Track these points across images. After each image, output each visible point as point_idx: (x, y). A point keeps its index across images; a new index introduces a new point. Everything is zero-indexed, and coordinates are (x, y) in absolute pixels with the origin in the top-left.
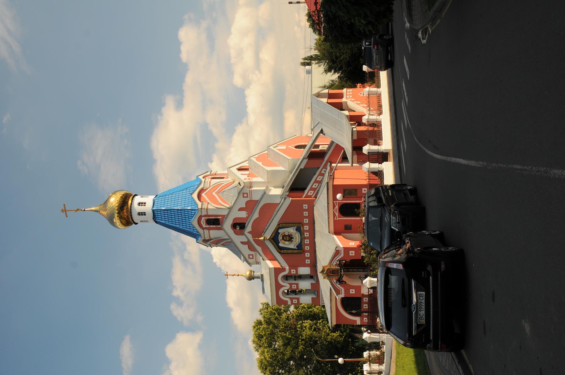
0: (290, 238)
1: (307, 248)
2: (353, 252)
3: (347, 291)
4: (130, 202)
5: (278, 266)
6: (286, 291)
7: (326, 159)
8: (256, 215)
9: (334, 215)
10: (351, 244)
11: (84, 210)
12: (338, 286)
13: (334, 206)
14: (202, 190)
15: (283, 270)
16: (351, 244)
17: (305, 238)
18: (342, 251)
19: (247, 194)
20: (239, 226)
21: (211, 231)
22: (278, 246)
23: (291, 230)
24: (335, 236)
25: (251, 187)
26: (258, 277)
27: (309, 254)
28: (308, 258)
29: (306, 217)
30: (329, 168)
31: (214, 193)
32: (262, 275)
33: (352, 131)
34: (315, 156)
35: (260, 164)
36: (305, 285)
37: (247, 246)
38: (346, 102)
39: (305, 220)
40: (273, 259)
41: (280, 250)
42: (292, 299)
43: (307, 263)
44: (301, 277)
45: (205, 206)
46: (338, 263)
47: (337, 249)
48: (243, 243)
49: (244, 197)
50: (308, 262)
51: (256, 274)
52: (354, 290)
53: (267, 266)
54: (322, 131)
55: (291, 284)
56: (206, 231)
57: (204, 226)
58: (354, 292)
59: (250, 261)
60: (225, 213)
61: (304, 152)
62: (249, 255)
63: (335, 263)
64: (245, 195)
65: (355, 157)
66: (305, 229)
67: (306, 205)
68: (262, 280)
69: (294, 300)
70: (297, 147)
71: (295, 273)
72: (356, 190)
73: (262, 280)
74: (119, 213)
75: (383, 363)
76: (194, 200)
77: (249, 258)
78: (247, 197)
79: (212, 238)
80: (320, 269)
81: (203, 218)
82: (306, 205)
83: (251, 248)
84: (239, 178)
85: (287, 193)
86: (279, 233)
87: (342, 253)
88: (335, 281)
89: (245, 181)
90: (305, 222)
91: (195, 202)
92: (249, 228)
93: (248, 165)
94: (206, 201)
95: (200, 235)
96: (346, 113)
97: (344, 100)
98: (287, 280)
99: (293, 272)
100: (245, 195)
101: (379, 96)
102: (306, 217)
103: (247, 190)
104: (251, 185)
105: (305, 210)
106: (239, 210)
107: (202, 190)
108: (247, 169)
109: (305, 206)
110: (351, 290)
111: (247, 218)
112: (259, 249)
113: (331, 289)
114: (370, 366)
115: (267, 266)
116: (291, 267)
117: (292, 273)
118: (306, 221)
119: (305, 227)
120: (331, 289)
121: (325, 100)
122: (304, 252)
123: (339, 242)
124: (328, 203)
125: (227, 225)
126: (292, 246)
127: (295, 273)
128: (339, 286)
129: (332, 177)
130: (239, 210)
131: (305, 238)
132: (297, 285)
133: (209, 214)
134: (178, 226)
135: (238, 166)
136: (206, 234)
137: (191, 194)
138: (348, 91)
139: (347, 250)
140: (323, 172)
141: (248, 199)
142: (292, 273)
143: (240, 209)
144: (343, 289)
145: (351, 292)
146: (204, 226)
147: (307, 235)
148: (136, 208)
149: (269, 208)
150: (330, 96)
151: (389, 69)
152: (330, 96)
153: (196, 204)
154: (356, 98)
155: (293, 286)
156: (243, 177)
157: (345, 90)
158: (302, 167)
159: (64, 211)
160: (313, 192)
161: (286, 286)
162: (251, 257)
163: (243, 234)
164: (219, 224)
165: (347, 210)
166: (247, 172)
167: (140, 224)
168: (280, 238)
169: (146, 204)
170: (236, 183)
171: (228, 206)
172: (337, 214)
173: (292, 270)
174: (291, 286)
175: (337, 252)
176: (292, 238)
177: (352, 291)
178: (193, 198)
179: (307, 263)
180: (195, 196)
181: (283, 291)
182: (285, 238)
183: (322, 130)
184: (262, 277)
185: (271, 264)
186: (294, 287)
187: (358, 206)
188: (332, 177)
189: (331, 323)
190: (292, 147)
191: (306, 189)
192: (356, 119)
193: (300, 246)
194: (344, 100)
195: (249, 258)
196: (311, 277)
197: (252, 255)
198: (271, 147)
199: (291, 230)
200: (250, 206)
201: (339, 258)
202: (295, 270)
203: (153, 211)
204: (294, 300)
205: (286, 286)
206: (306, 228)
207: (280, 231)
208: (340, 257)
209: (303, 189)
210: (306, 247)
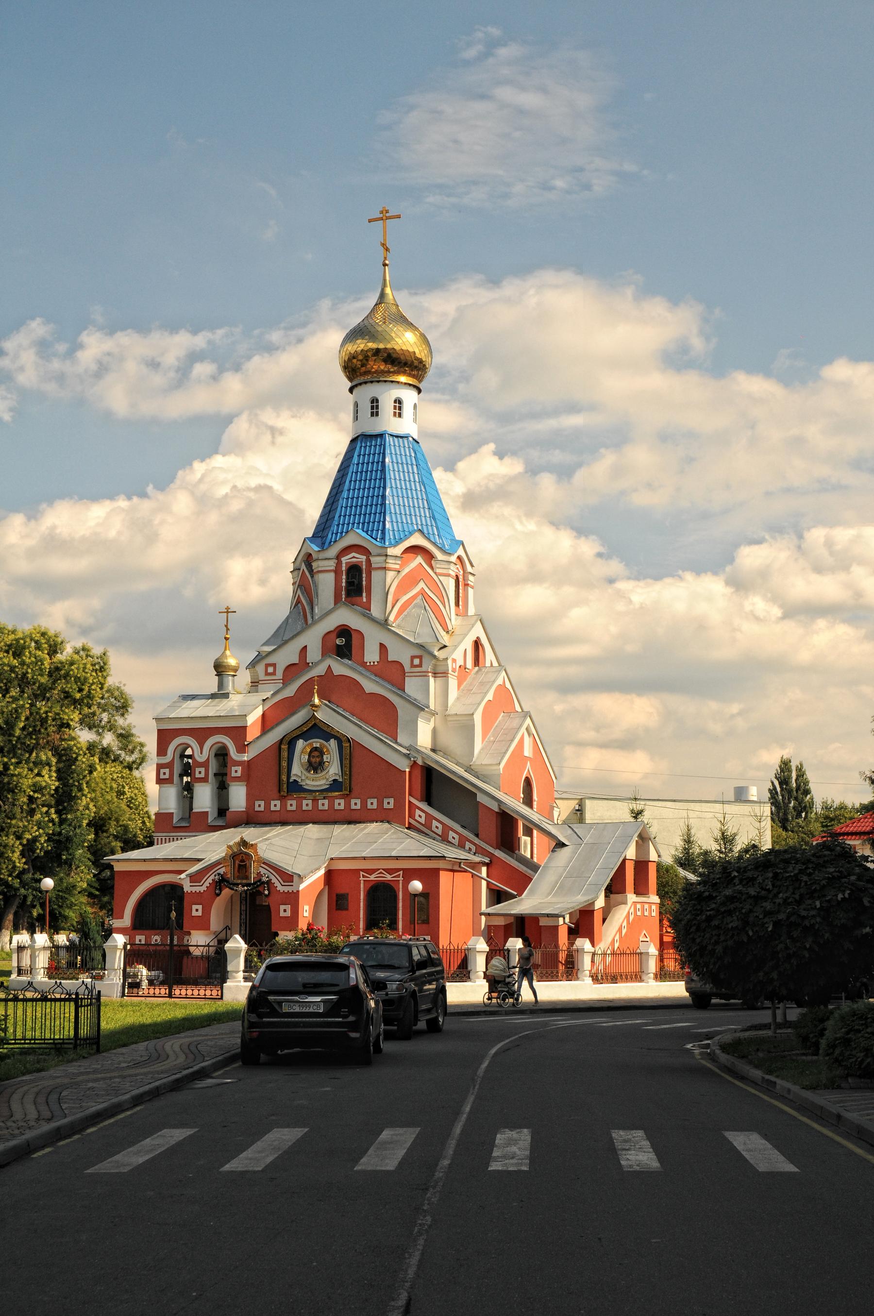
0: (316, 765)
1: (292, 805)
2: (288, 914)
3: (198, 898)
4: (403, 379)
5: (250, 738)
6: (189, 752)
7: (498, 853)
8: (370, 686)
9: (370, 872)
10: (306, 908)
11: (385, 265)
12: (209, 880)
13: (390, 871)
14: (429, 556)
15: (242, 748)
16: (306, 908)
17: (315, 801)
18: (290, 889)
19: (420, 665)
20: (344, 644)
21: (332, 575)
22: (298, 737)
23: (333, 770)
24: (322, 872)
25: (435, 674)
26: (221, 685)
27: (278, 808)
28: (268, 805)
29: (364, 804)
30: (477, 859)
31: (422, 585)
32: (226, 696)
33: (557, 916)
34: (505, 829)
35: (490, 696)
36: (204, 798)
38: (625, 903)
39: (358, 801)
40: (267, 724)
41: (290, 741)
42: (170, 765)
43: (257, 803)
44: (222, 788)
45: (392, 564)
46: (264, 879)
47: (295, 878)
49: (413, 658)
50: (260, 806)
51: (229, 682)
52: (200, 913)
53: (247, 706)
54: (561, 845)
55: (205, 764)
56: (332, 564)
57: (344, 560)
58: (194, 913)
59: (260, 668)
60: (375, 611)
61: (515, 804)
62: (274, 665)
63: (263, 871)
64: (416, 661)
65: (501, 922)
66: (337, 801)
67: (391, 806)
68: (213, 696)
69: (167, 771)
70: (528, 782)
71: (234, 774)
72: (426, 922)
73: (213, 696)
74: (377, 352)
75: (50, 978)
76: (407, 537)
77: (267, 666)
78: (413, 666)
79: (316, 577)
80: (249, 834)
81: (363, 558)
82: (391, 806)
83: (292, 671)
84: (456, 647)
85: (420, 762)
86: (327, 740)
87: (286, 889)
88: (222, 871)
89: (450, 662)
90: (353, 801)
91: (401, 540)
92: (340, 668)
93: (488, 664)
94: (403, 566)
95: (323, 547)
96: (600, 903)
97: (631, 897)
98: (216, 755)
99: (236, 771)
100: (416, 661)
101: (637, 977)
102: (364, 804)
103: (428, 666)
104: (441, 673)
105: (380, 803)
106: (381, 644)
107: (429, 556)
108: (477, 661)
109: (389, 803)
110: (200, 907)
111: (363, 664)
112: (290, 691)
113: (199, 860)
114: (44, 948)
115: (247, 706)
116: (248, 766)
117: (234, 769)
118: (356, 804)
119: (342, 801)
120: (199, 860)
121: (631, 853)
122: (282, 798)
123: (311, 881)
124: (397, 858)
125: (346, 617)
126: (297, 770)
127: (234, 774)
128: (210, 880)
129: (456, 867)
130: (381, 644)
131: (315, 801)
132: (205, 780)
133: (374, 574)
134: (345, 494)
135: (484, 641)
136: (325, 564)
137: (421, 531)
138: (654, 907)
139: (293, 899)
140: (468, 845)
141: (407, 668)
142: (234, 769)
143: (383, 648)
144: (202, 889)
145: (194, 907)
146: (344, 560)
147: (323, 804)
148: (388, 395)
149: (385, 716)
150: (641, 866)
151: (690, 1001)
152: (641, 866)
153: (397, 543)
154: (635, 924)
155: (203, 770)
156: (459, 654)
157: (656, 899)
158: (480, 798)
159: (385, 216)
160: (423, 820)
161: (202, 753)
162: (271, 670)
163: (325, 653)
164: (348, 594)
165: (382, 900)
166: (470, 664)
167: (351, 398)
168: (317, 743)
169: (397, 419)
170: (445, 639)
171: (392, 618)
172: (372, 877)
173: (239, 769)
174: (201, 765)
175: (288, 877)
176: (316, 771)
177: (197, 910)
178: (411, 534)
180: (417, 540)
181: (188, 746)
182: (316, 753)
183: (563, 845)
184: (221, 695)
185: (254, 717)
186: (200, 772)
187: (393, 926)
188: (456, 868)
189: (118, 860)
190: (528, 770)
191: (430, 804)
192: (583, 923)
193: (295, 788)
194: (631, 897)
195: (267, 666)
196: (222, 811)
197: (274, 673)
198: (528, 720)
199: (333, 770)
200: (392, 673)
201: (274, 880)
202: (239, 774)
203: (381, 436)
204: (167, 771)
205: (202, 753)
206: (340, 804)
207: (333, 743)
208: (277, 884)
209: (428, 798)
210: (294, 802)
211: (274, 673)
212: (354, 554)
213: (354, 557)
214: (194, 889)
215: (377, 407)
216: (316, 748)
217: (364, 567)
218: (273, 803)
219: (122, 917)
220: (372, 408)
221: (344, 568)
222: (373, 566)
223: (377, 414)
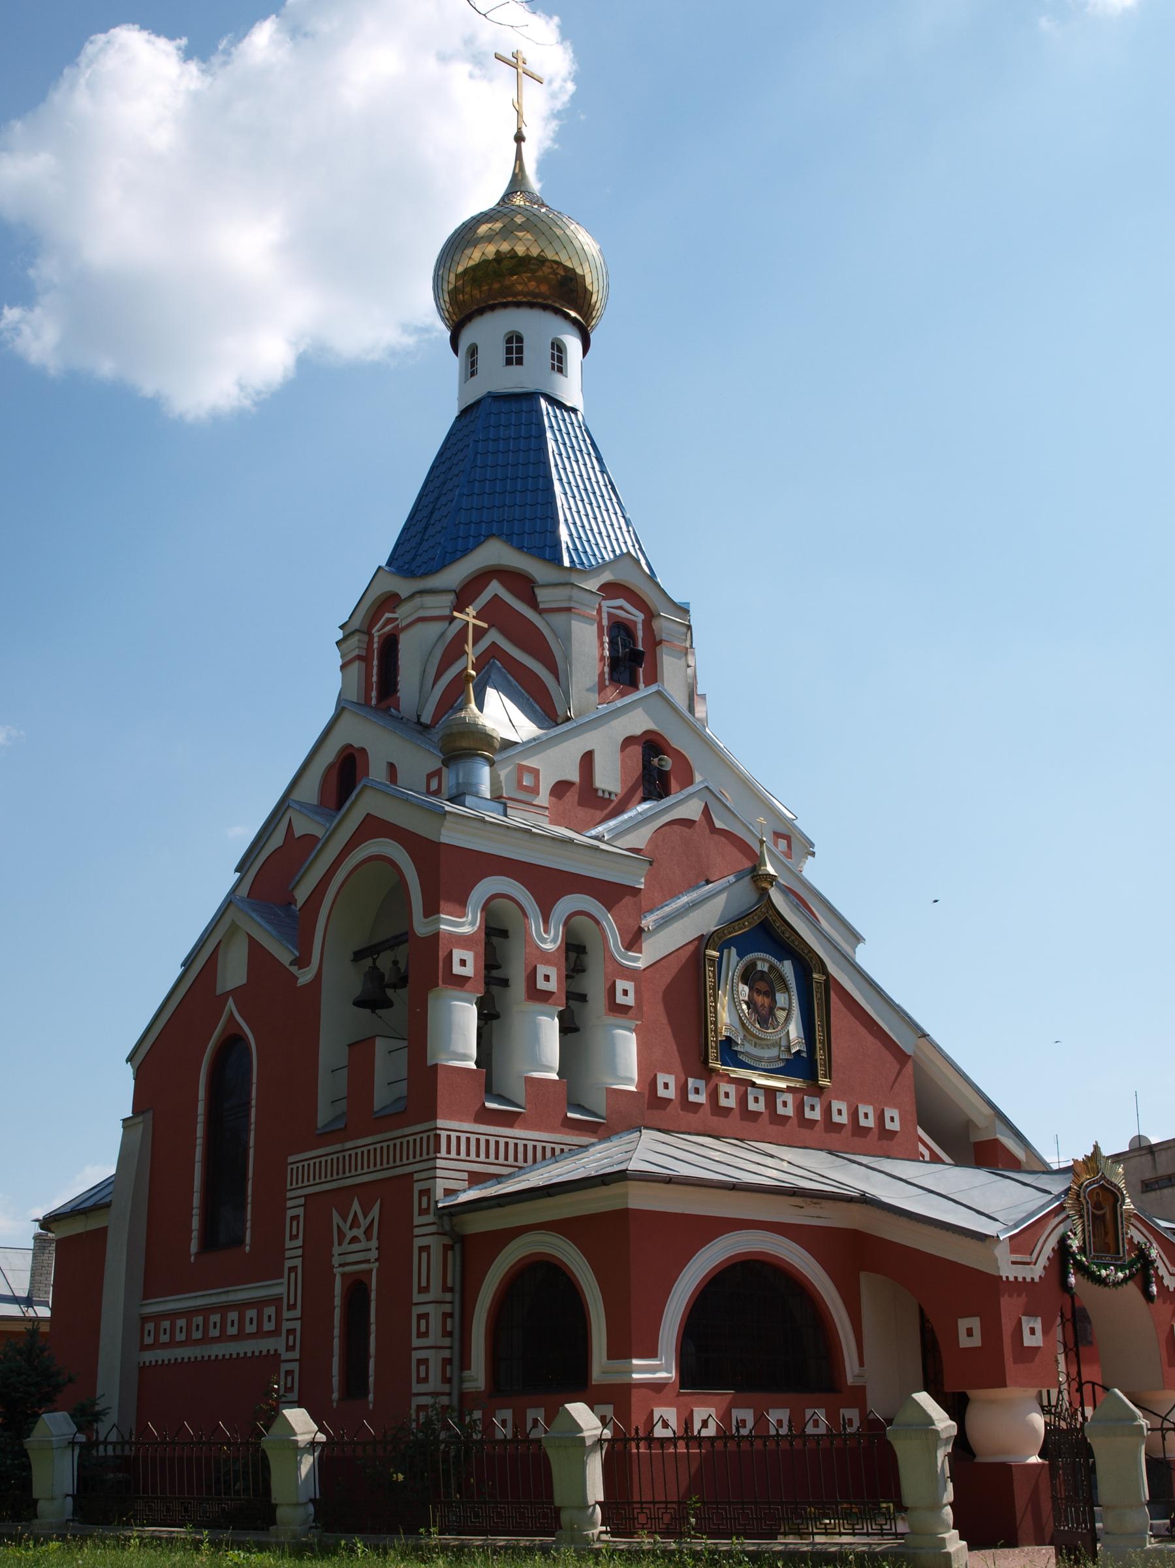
37: (574, 776)
48: (588, 759)
50: (667, 1086)
62: (535, 773)
195: (521, 769)
197: (535, 790)
199: (794, 1031)
212: (621, 602)
213: (621, 608)
215: (560, 360)
216: (762, 972)
217: (640, 634)
221: (605, 622)
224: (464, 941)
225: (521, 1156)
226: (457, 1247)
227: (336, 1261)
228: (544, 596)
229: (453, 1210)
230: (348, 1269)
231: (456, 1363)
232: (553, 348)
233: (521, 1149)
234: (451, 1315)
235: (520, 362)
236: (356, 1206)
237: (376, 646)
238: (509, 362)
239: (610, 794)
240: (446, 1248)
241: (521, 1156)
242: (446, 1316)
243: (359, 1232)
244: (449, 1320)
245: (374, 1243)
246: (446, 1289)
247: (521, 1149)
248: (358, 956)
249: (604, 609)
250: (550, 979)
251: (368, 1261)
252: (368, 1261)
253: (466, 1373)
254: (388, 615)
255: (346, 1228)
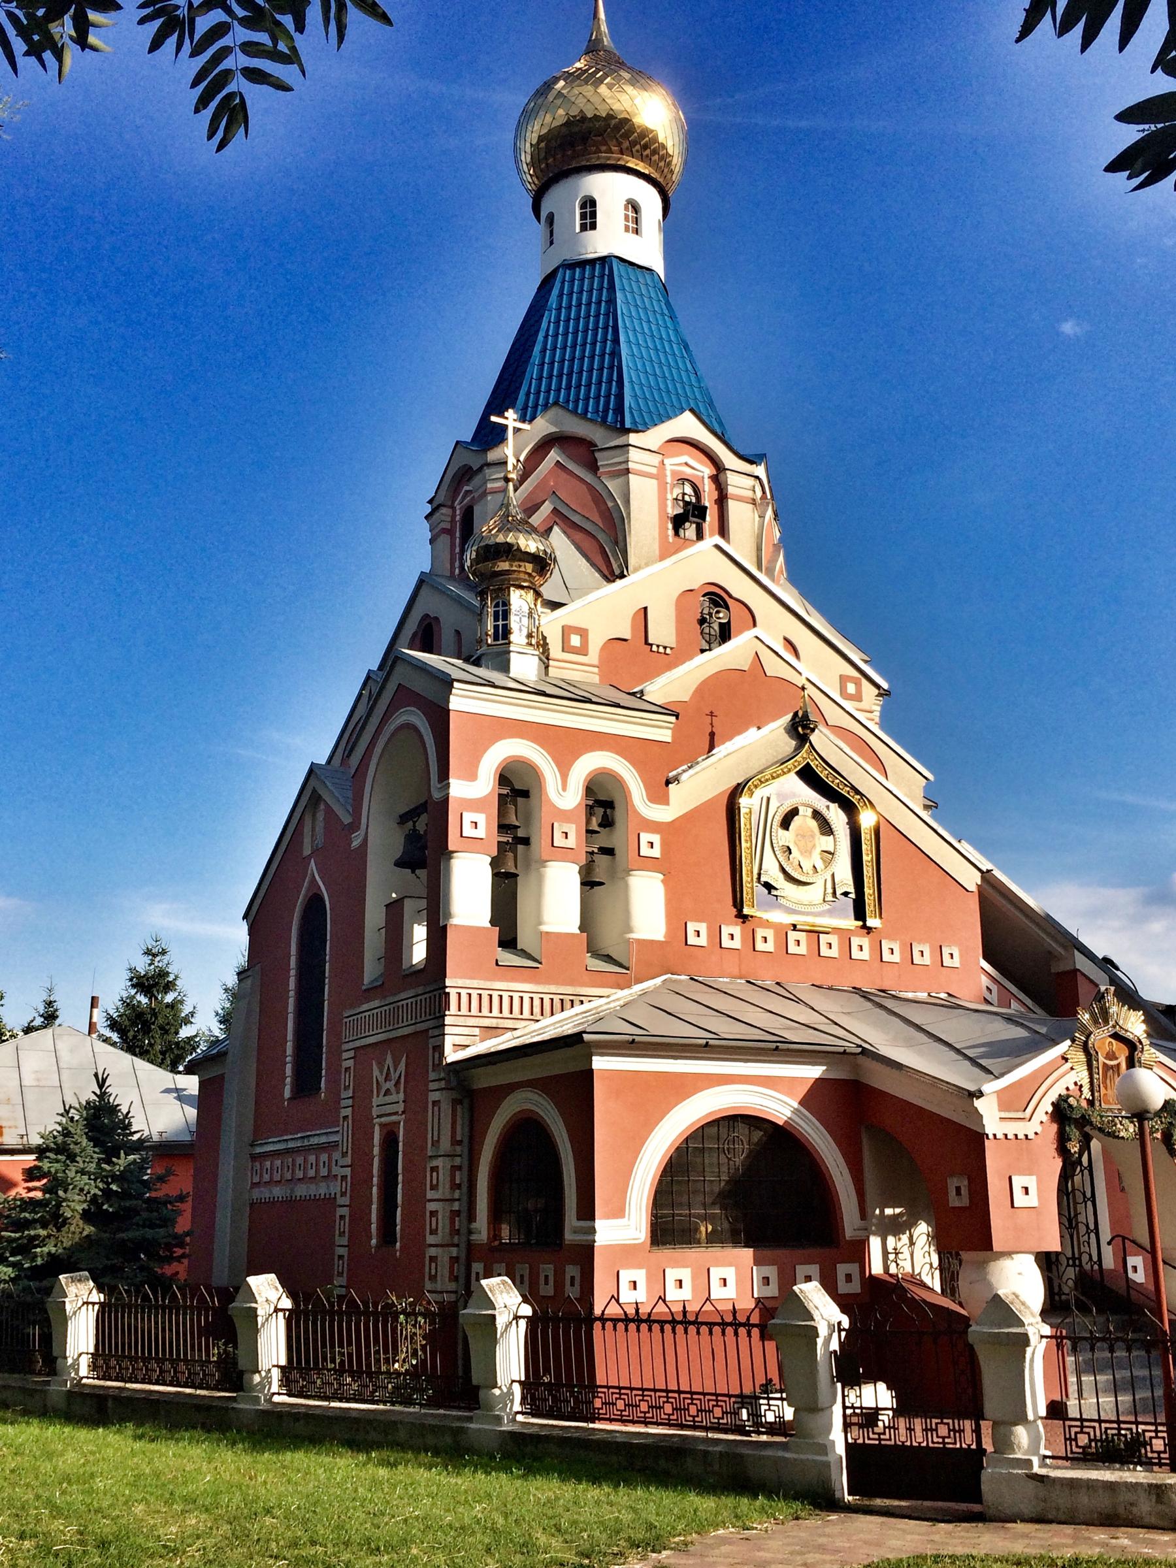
19: (857, 697)
62: (583, 633)
77: (566, 631)
99: (651, 845)
162: (575, 640)
179: (692, 927)
195: (566, 631)
197: (583, 650)
211: (583, 650)
214: (1012, 1129)
215: (637, 221)
218: (726, 931)
219: (619, 1212)
220: (627, 218)
221: (669, 480)
222: (731, 490)
223: (637, 231)
224: (475, 805)
225: (537, 1010)
226: (466, 1102)
227: (375, 1112)
228: (603, 460)
229: (458, 1067)
230: (383, 1120)
231: (464, 1215)
232: (626, 209)
233: (537, 1003)
234: (459, 1168)
235: (593, 226)
236: (389, 1061)
237: (458, 518)
238: (584, 228)
239: (665, 648)
240: (455, 1102)
241: (537, 1010)
242: (454, 1169)
243: (390, 1085)
244: (457, 1173)
245: (401, 1096)
246: (455, 1142)
247: (537, 1003)
248: (404, 819)
249: (669, 468)
250: (570, 835)
251: (396, 1113)
252: (396, 1113)
253: (474, 1225)
254: (466, 488)
255: (381, 1079)
